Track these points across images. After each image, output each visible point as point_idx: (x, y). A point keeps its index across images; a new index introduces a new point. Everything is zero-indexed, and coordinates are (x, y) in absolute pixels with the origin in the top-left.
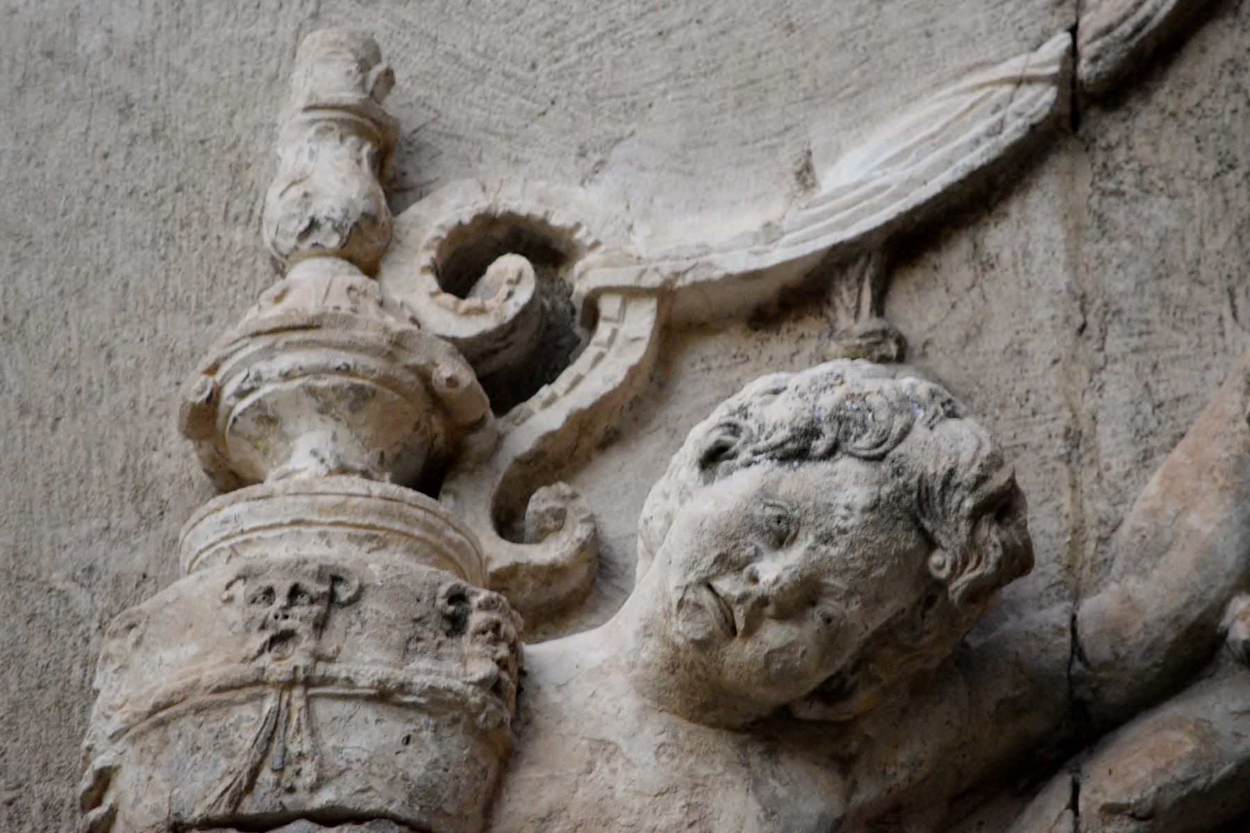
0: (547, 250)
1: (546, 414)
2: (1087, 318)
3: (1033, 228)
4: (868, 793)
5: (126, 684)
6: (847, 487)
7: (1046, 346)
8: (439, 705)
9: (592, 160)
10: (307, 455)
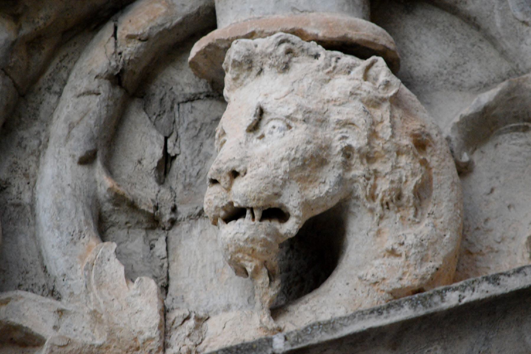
4: (27, 30)
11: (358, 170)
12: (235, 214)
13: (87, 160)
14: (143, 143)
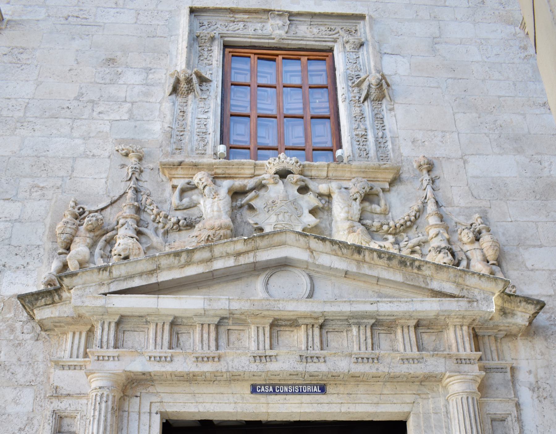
0: (83, 209)
1: (83, 216)
2: (111, 214)
3: (108, 210)
5: (57, 227)
6: (94, 219)
8: (72, 228)
9: (87, 205)
10: (69, 217)
11: (131, 251)
12: (115, 255)
13: (101, 249)
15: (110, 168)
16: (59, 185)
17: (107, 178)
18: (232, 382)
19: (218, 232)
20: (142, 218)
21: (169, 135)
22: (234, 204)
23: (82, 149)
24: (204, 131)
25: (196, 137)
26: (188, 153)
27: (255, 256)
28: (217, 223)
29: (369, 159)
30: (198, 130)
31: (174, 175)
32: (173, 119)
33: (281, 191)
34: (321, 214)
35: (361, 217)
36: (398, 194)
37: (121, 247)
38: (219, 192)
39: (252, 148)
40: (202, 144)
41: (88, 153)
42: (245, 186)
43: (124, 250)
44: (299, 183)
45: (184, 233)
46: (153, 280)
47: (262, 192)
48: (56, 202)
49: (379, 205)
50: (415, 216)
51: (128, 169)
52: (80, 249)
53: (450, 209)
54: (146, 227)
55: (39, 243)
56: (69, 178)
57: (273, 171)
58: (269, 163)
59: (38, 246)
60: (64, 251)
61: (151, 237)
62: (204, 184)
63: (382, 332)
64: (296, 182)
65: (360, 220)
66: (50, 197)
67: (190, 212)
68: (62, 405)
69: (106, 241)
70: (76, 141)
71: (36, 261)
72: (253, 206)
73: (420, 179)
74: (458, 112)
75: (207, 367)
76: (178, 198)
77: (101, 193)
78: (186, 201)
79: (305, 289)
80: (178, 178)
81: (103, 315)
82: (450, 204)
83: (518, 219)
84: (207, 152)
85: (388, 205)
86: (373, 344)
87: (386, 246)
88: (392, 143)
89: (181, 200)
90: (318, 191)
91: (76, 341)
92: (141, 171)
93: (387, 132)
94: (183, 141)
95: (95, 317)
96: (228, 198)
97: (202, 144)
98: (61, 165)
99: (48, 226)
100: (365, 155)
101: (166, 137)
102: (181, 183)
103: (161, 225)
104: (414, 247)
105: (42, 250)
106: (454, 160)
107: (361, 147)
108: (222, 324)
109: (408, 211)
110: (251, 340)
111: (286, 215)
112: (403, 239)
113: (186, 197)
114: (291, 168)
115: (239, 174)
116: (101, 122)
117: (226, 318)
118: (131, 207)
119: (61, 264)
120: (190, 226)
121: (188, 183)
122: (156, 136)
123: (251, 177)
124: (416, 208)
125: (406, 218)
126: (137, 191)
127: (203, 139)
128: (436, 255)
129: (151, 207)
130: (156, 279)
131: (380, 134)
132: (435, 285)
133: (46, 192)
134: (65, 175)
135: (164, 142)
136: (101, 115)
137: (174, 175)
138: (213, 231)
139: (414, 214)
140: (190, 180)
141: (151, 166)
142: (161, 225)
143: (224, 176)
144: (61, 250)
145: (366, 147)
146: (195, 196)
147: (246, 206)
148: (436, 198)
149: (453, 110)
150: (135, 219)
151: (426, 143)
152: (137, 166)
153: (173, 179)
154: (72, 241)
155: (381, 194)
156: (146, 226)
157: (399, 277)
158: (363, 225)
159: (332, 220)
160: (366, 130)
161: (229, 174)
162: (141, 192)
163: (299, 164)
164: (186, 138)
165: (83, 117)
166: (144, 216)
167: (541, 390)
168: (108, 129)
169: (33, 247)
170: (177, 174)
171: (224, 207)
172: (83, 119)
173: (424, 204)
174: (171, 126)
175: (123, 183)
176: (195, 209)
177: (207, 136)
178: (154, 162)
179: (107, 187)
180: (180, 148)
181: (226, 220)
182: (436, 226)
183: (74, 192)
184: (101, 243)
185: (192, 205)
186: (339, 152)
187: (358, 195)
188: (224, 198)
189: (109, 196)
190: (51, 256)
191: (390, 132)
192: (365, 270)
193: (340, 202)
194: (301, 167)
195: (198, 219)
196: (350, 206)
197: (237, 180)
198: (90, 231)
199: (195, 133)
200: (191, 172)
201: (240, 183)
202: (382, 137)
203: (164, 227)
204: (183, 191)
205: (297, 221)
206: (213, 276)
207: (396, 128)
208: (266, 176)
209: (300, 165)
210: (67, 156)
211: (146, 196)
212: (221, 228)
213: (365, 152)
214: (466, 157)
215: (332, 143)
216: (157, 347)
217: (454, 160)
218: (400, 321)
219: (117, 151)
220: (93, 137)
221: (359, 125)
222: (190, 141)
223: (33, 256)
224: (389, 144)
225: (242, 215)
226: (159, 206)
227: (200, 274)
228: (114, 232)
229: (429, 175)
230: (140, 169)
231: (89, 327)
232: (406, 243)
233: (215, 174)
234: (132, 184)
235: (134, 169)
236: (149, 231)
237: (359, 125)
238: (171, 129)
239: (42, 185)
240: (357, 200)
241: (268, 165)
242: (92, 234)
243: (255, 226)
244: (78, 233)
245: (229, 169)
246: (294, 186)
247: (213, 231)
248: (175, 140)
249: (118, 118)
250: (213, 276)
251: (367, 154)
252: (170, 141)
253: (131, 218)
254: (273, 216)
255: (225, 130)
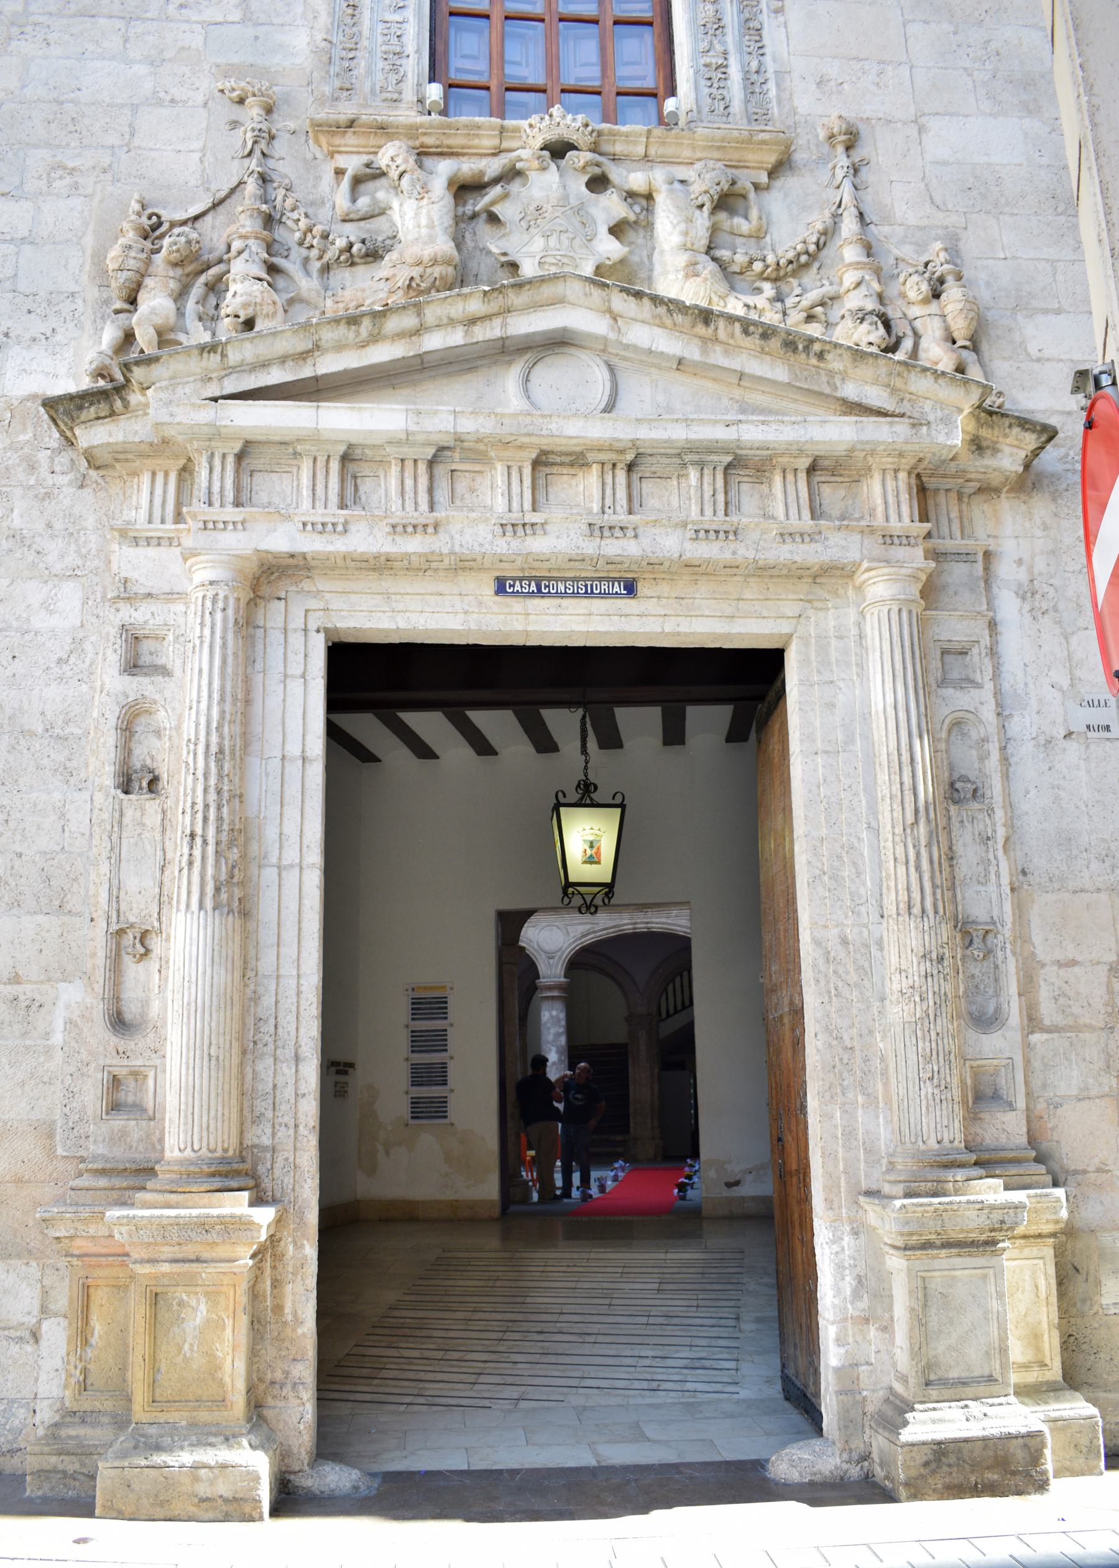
0: (159, 217)
1: (158, 233)
3: (209, 218)
6: (183, 239)
7: (209, 230)
8: (140, 259)
10: (131, 234)
11: (258, 308)
12: (228, 316)
13: (197, 303)
14: (212, 301)
15: (208, 129)
16: (106, 165)
17: (203, 150)
18: (460, 572)
19: (429, 270)
20: (277, 237)
21: (325, 59)
22: (460, 210)
23: (148, 86)
24: (398, 49)
25: (381, 64)
26: (365, 100)
27: (504, 325)
28: (427, 253)
29: (731, 119)
30: (384, 48)
31: (339, 146)
32: (333, 23)
33: (555, 186)
34: (631, 235)
35: (710, 242)
36: (786, 195)
37: (239, 300)
38: (429, 186)
39: (493, 88)
40: (393, 78)
41: (162, 95)
42: (482, 173)
43: (246, 305)
44: (589, 169)
45: (361, 270)
46: (307, 372)
47: (515, 187)
48: (101, 201)
49: (746, 218)
50: (817, 244)
51: (245, 133)
52: (156, 302)
53: (886, 229)
54: (286, 257)
55: (74, 288)
56: (126, 149)
57: (539, 142)
58: (531, 126)
59: (73, 294)
60: (126, 306)
61: (296, 278)
62: (401, 169)
63: (745, 479)
64: (584, 167)
65: (709, 249)
66: (89, 191)
67: (372, 226)
68: (140, 615)
69: (206, 285)
70: (136, 68)
71: (71, 325)
72: (497, 216)
73: (830, 165)
74: (914, 21)
75: (413, 545)
76: (348, 196)
77: (193, 183)
78: (363, 202)
79: (601, 391)
80: (346, 152)
81: (210, 440)
82: (888, 219)
83: (1019, 254)
84: (403, 96)
85: (764, 220)
86: (726, 504)
87: (758, 306)
88: (778, 85)
89: (354, 200)
90: (626, 188)
91: (159, 491)
92: (272, 138)
93: (768, 59)
94: (354, 72)
95: (196, 444)
96: (449, 199)
97: (393, 78)
98: (107, 120)
99: (89, 252)
100: (722, 109)
101: (320, 61)
102: (353, 164)
103: (314, 253)
104: (812, 307)
105: (80, 302)
106: (899, 125)
107: (713, 91)
108: (440, 459)
109: (803, 234)
110: (496, 491)
111: (564, 237)
112: (792, 290)
113: (365, 195)
114: (575, 137)
115: (469, 148)
116: (185, 26)
117: (448, 448)
118: (256, 215)
119: (120, 334)
120: (373, 255)
121: (368, 166)
122: (298, 61)
123: (494, 155)
124: (819, 226)
125: (799, 247)
126: (264, 179)
127: (395, 68)
128: (855, 328)
129: (295, 215)
130: (312, 369)
131: (754, 65)
132: (850, 391)
133: (80, 180)
134: (117, 142)
135: (315, 74)
136: (183, 11)
137: (339, 146)
138: (420, 269)
139: (814, 239)
140: (371, 157)
141: (292, 125)
142: (314, 253)
143: (439, 150)
144: (119, 305)
145: (724, 92)
146: (381, 192)
147: (484, 216)
148: (861, 205)
149: (902, 15)
150: (264, 240)
151: (846, 86)
152: (264, 126)
153: (337, 156)
154: (139, 285)
155: (752, 195)
156: (286, 253)
157: (780, 373)
158: (714, 259)
159: (654, 248)
160: (725, 53)
161: (448, 147)
162: (272, 181)
163: (590, 128)
164: (361, 66)
165: (148, 15)
166: (280, 233)
167: (1037, 596)
168: (201, 44)
169: (62, 297)
170: (345, 145)
171: (441, 217)
172: (148, 19)
173: (836, 217)
174: (329, 38)
175: (236, 162)
176: (382, 219)
177: (404, 61)
178: (297, 118)
179: (203, 171)
180: (349, 86)
181: (444, 245)
182: (857, 265)
183: (138, 181)
184: (197, 290)
185: (376, 212)
186: (670, 104)
187: (705, 199)
188: (442, 199)
189: (208, 189)
190: (99, 315)
191: (774, 60)
192: (717, 357)
193: (670, 212)
194: (594, 134)
195: (389, 242)
196: (690, 220)
197: (465, 159)
198: (175, 265)
199: (379, 55)
200: (373, 141)
201: (473, 166)
202: (757, 72)
203: (320, 258)
204: (357, 181)
205: (584, 251)
206: (422, 363)
207: (786, 54)
208: (524, 153)
209: (593, 131)
210: (119, 101)
211: (283, 192)
212: (435, 262)
213: (722, 103)
214: (923, 120)
215: (657, 82)
216: (318, 503)
217: (899, 125)
218: (779, 459)
219: (222, 91)
220: (170, 60)
221: (711, 43)
222: (369, 72)
223: (63, 315)
224: (771, 86)
225: (475, 233)
226: (310, 211)
227: (398, 360)
228: (220, 268)
229: (848, 157)
230: (269, 133)
231: (182, 462)
232: (798, 299)
233: (422, 146)
234: (253, 164)
235: (256, 133)
236: (291, 266)
237: (711, 43)
238: (329, 45)
239: (71, 165)
240: (705, 209)
241: (528, 130)
242: (179, 271)
243: (503, 259)
244: (151, 270)
245: (449, 136)
246: (580, 175)
247: (420, 269)
248: (337, 69)
249: (220, 19)
250: (422, 363)
251: (726, 108)
252: (328, 72)
253: (257, 238)
254: (537, 238)
255: (440, 48)
